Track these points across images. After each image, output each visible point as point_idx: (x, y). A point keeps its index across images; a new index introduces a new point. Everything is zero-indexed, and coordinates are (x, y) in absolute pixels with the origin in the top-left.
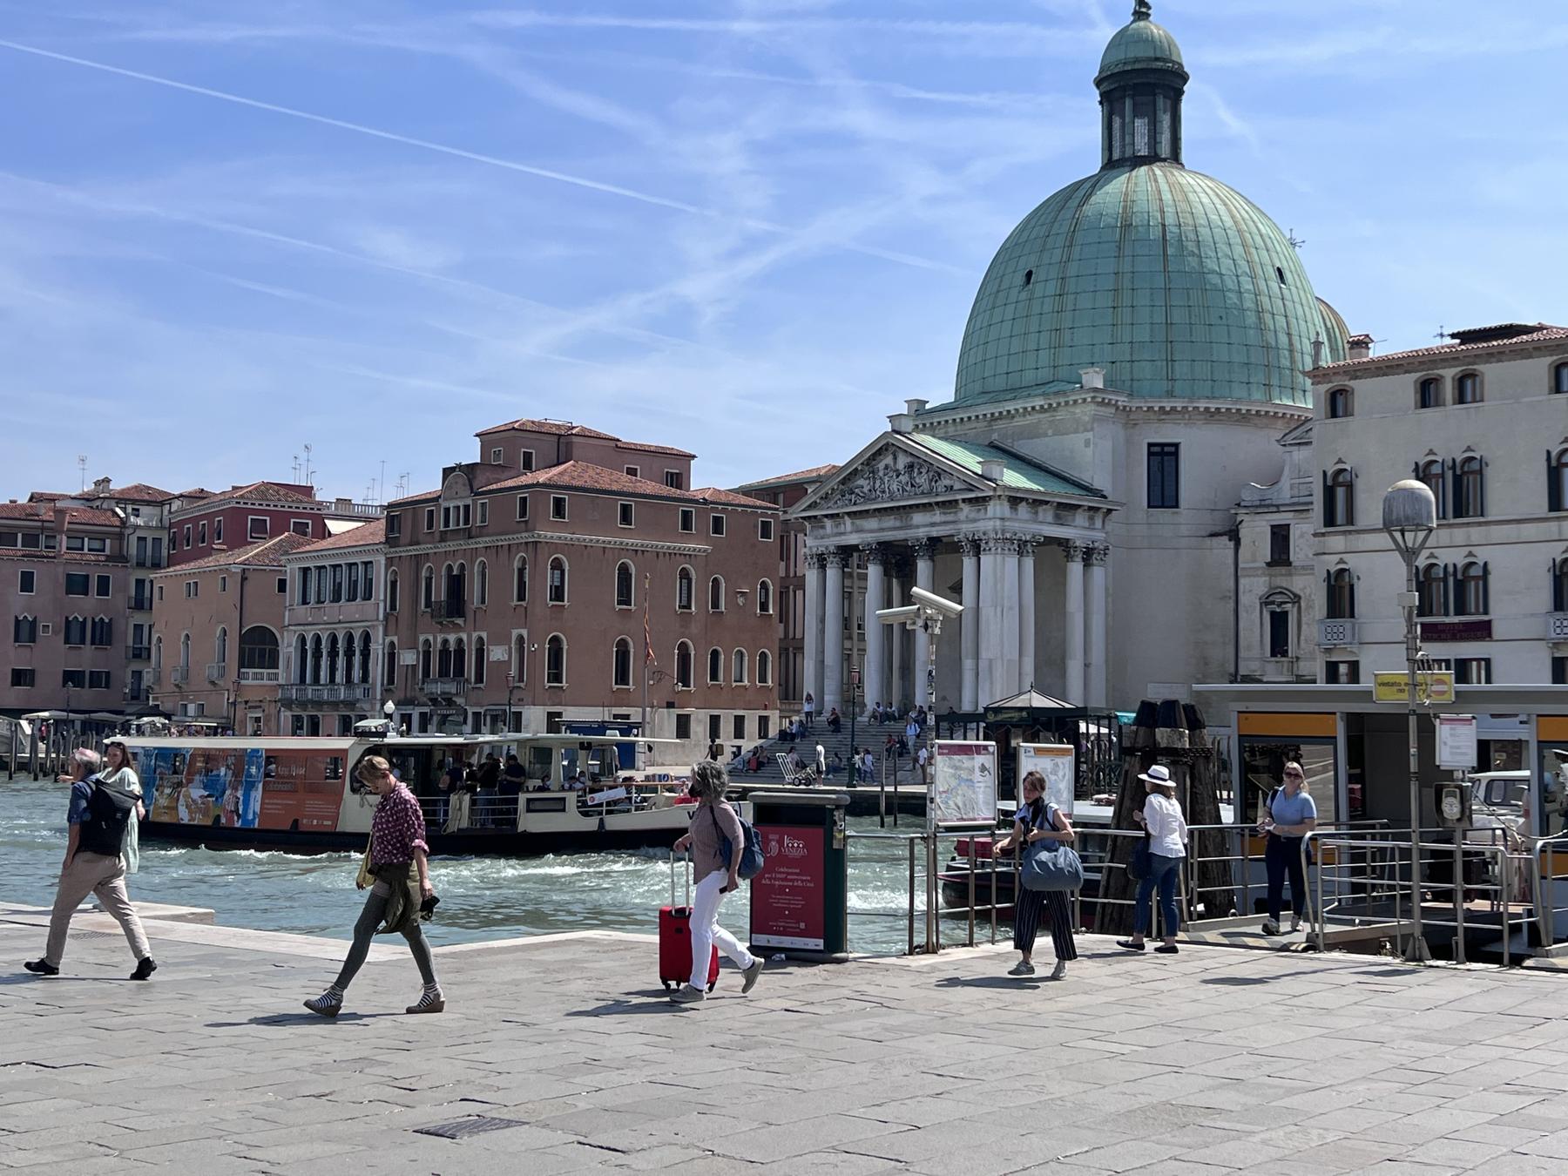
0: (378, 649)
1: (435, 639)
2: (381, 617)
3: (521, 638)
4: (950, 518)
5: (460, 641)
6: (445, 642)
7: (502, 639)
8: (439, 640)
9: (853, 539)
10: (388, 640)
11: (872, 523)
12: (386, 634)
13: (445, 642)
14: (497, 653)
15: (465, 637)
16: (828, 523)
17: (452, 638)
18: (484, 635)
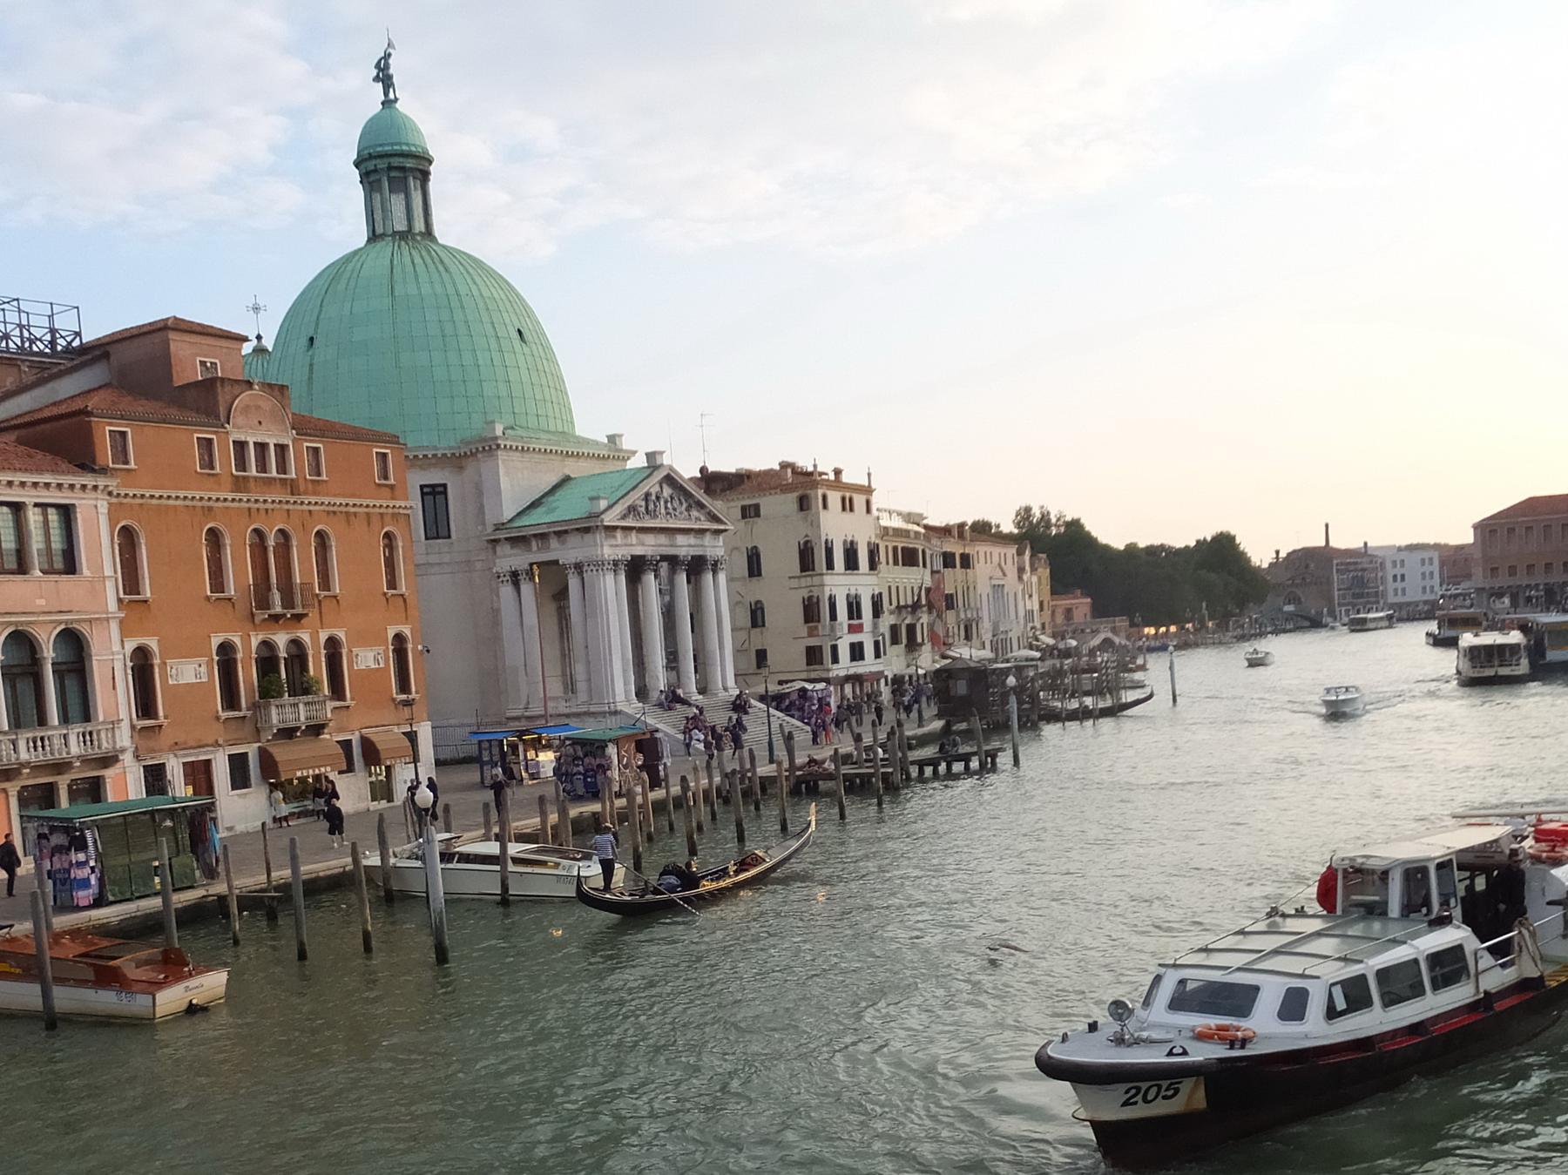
0: (110, 659)
1: (246, 640)
2: (112, 605)
3: (399, 639)
4: (699, 542)
5: (296, 643)
6: (267, 645)
7: (366, 638)
8: (255, 643)
9: (639, 551)
10: (130, 645)
11: (650, 539)
12: (125, 633)
13: (267, 645)
14: (366, 659)
15: (305, 637)
16: (619, 534)
17: (281, 639)
18: (341, 635)
